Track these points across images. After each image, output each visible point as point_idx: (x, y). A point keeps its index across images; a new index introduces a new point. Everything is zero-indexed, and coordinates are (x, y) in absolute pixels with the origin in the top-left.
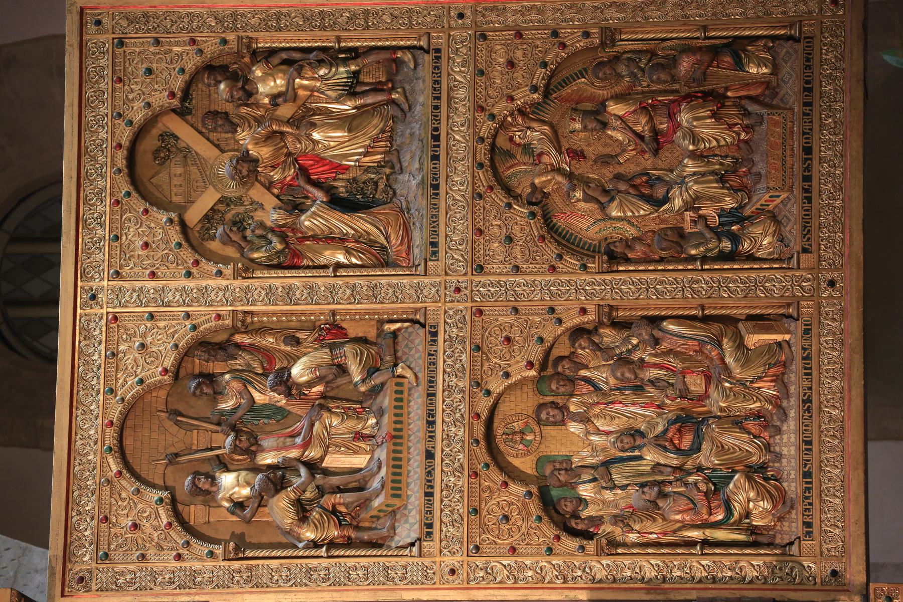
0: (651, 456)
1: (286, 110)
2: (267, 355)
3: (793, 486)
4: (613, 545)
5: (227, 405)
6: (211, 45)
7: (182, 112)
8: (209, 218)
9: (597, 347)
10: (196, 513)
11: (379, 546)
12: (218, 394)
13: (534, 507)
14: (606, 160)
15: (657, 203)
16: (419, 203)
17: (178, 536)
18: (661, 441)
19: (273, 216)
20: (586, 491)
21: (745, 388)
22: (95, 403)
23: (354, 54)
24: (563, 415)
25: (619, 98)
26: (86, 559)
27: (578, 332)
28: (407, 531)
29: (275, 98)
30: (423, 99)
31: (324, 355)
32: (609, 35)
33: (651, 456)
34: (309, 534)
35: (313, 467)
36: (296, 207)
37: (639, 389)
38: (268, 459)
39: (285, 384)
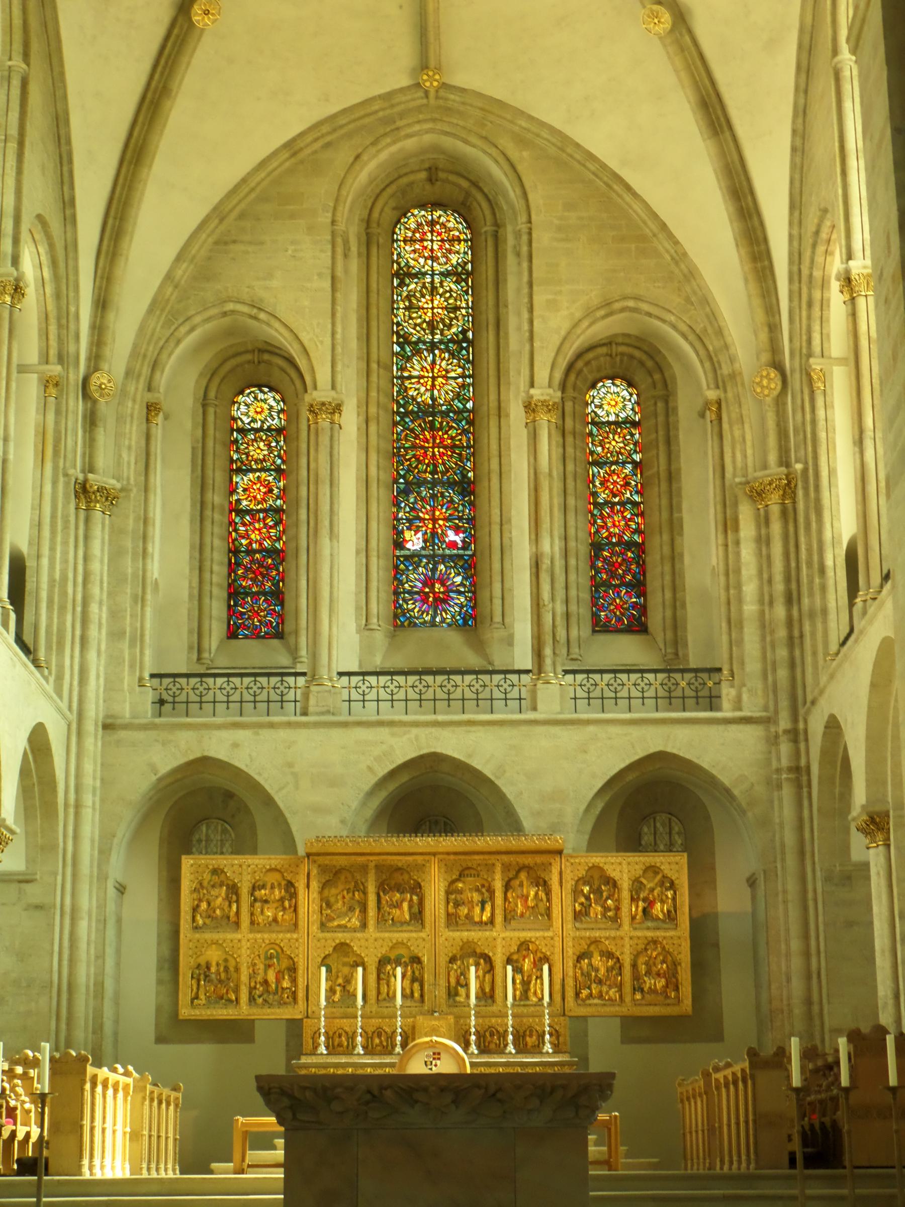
0: (593, 974)
1: (664, 898)
2: (613, 895)
3: (588, 1002)
4: (575, 966)
5: (603, 887)
6: (676, 882)
7: (663, 876)
8: (641, 883)
9: (615, 963)
10: (581, 882)
11: (575, 918)
12: (605, 885)
13: (583, 951)
14: (655, 964)
15: (645, 975)
16: (644, 926)
17: (576, 878)
18: (596, 976)
19: (641, 896)
20: (586, 961)
21: (607, 993)
22: (603, 860)
23: (676, 911)
24: (601, 956)
25: (667, 966)
26: (572, 861)
27: (618, 959)
28: (577, 925)
29: (667, 896)
30: (666, 926)
31: (612, 907)
32: (680, 964)
33: (593, 974)
34: (577, 905)
35: (590, 905)
36: (644, 900)
37: (607, 971)
38: (592, 896)
39: (607, 899)
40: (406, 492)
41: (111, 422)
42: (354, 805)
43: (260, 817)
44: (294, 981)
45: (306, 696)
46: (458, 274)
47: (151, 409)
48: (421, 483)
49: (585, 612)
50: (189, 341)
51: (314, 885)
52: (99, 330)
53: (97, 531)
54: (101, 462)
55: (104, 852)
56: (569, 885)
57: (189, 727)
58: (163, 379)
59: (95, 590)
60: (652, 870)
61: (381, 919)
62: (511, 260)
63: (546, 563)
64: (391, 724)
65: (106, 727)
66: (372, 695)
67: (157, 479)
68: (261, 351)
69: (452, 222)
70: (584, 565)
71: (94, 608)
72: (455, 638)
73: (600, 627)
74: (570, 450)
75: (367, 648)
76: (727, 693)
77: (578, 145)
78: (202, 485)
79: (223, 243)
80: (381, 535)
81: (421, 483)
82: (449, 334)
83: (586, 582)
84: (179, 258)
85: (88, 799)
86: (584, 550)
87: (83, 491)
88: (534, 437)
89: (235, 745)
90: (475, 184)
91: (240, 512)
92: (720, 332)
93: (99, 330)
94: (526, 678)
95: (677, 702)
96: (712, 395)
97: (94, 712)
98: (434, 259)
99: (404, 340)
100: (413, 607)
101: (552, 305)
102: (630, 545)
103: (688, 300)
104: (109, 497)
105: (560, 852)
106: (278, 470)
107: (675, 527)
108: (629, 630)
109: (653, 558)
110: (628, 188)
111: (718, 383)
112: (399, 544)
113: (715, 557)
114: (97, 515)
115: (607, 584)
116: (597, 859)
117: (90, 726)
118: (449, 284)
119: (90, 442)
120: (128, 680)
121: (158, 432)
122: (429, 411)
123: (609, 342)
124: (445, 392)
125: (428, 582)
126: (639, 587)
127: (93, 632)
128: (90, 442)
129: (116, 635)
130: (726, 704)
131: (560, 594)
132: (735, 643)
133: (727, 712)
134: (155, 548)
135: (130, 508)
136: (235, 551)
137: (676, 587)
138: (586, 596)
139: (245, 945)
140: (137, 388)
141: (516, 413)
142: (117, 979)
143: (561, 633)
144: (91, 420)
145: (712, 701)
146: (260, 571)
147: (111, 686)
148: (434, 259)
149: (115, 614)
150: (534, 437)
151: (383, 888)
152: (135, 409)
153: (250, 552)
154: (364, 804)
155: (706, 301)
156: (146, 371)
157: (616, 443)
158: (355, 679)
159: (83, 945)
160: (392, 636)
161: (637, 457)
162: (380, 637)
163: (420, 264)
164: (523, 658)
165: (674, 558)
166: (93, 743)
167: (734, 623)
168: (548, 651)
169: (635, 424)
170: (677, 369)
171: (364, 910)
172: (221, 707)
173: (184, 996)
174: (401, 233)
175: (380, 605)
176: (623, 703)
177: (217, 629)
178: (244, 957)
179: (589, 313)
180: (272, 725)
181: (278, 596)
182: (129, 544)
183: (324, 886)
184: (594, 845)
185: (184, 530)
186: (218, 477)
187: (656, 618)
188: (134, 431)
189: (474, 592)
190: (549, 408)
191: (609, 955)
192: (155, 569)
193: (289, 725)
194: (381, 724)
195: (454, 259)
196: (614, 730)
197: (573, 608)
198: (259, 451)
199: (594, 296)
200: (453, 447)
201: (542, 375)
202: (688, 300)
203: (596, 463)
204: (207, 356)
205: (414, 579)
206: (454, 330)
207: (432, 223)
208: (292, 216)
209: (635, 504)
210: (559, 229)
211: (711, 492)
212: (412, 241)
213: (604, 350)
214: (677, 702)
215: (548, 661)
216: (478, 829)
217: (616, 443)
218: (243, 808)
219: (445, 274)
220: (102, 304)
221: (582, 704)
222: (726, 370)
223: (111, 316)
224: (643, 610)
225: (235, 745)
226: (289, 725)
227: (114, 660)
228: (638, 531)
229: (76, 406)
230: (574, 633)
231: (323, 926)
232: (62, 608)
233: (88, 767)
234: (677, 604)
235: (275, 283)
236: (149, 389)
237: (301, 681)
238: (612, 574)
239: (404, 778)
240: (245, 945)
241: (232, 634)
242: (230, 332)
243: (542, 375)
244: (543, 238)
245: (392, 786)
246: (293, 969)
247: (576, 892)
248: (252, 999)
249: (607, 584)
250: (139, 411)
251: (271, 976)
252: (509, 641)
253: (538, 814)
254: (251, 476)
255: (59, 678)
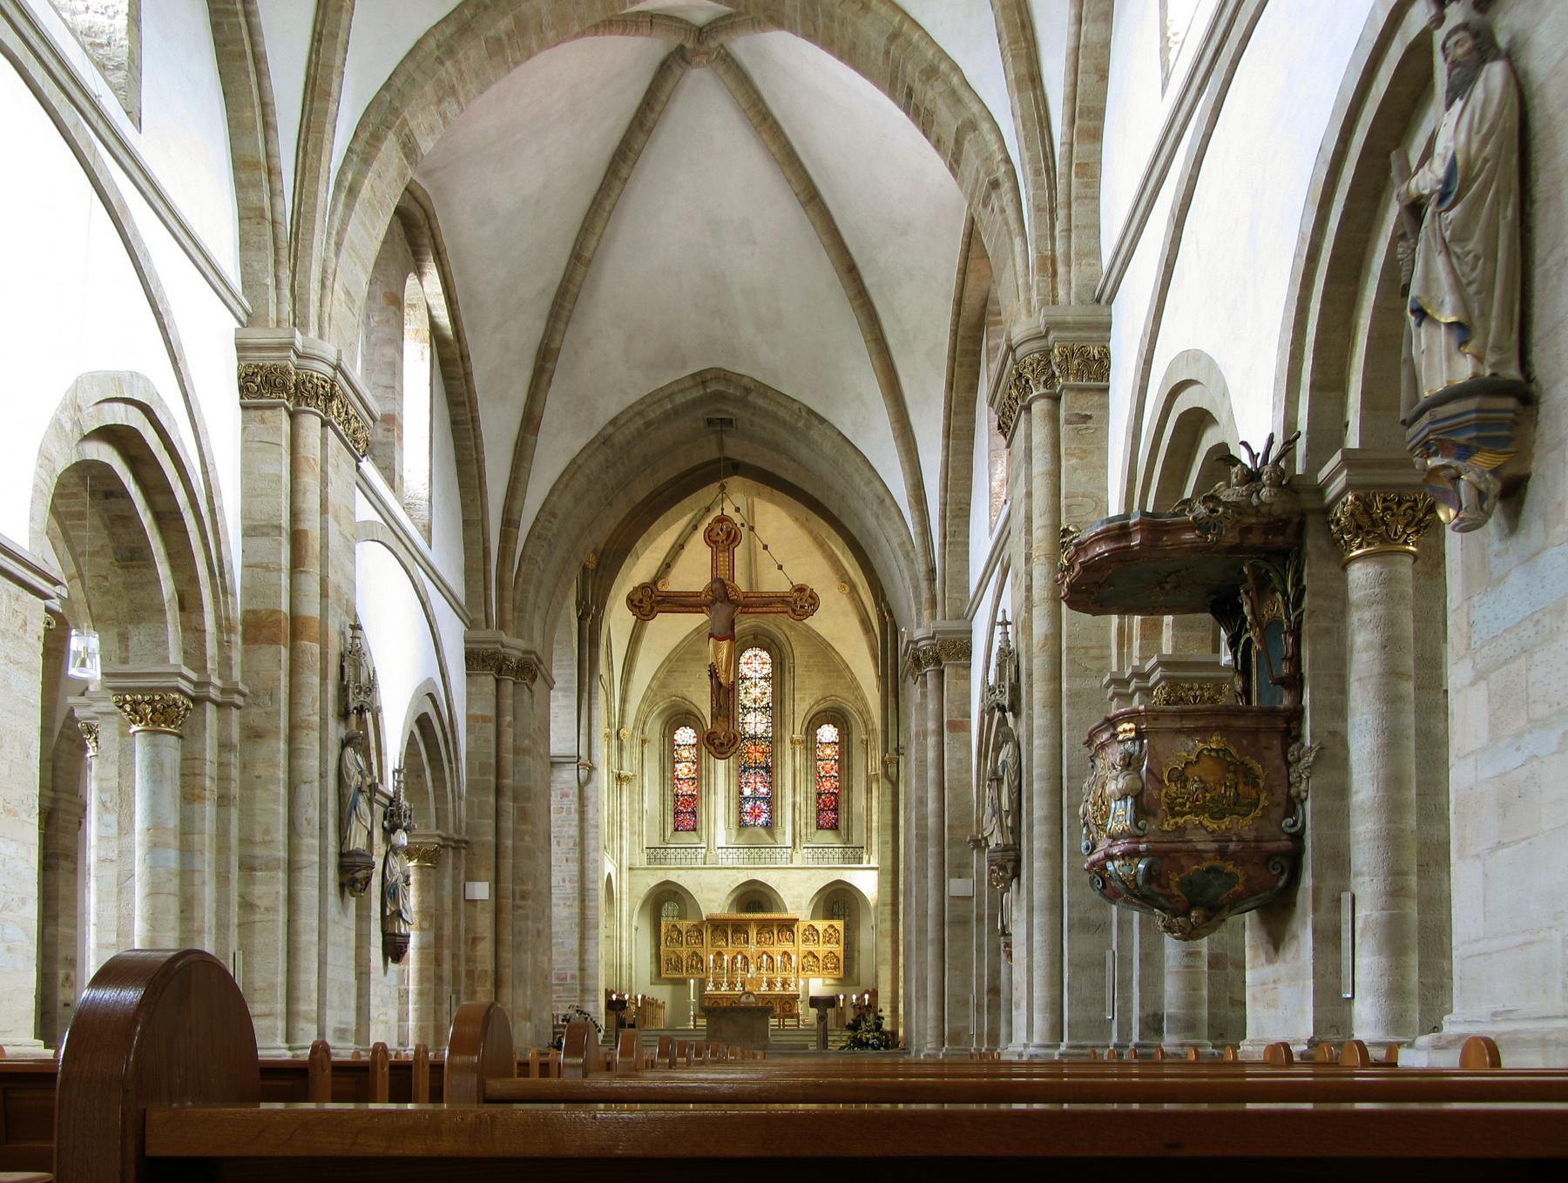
40: (744, 771)
41: (628, 748)
42: (724, 899)
43: (684, 896)
44: (702, 965)
45: (705, 857)
46: (765, 678)
47: (644, 742)
48: (750, 768)
49: (814, 822)
50: (656, 712)
51: (709, 931)
52: (623, 711)
53: (624, 793)
54: (625, 765)
55: (631, 916)
56: (801, 931)
57: (661, 869)
58: (647, 728)
59: (624, 817)
60: (831, 926)
61: (733, 942)
62: (787, 674)
63: (798, 805)
64: (738, 868)
65: (630, 869)
66: (731, 856)
67: (646, 770)
68: (686, 714)
69: (765, 655)
70: (814, 803)
71: (624, 824)
72: (762, 832)
73: (819, 827)
74: (809, 756)
75: (728, 835)
76: (865, 857)
77: (814, 631)
78: (663, 770)
79: (671, 671)
80: (734, 789)
81: (750, 768)
82: (763, 704)
83: (814, 809)
84: (653, 679)
85: (624, 897)
86: (814, 796)
87: (619, 778)
88: (794, 754)
89: (679, 876)
90: (773, 641)
91: (678, 779)
92: (868, 712)
93: (623, 711)
94: (789, 850)
95: (847, 860)
96: (864, 737)
97: (625, 864)
98: (756, 671)
99: (744, 707)
100: (747, 819)
101: (802, 699)
102: (833, 793)
103: (856, 698)
104: (628, 779)
105: (797, 920)
106: (693, 762)
107: (850, 788)
108: (831, 828)
109: (843, 799)
110: (834, 649)
111: (867, 732)
112: (741, 793)
113: (864, 802)
114: (624, 786)
115: (823, 810)
116: (812, 923)
117: (624, 869)
118: (762, 682)
119: (621, 757)
120: (637, 850)
121: (646, 750)
122: (754, 737)
123: (825, 711)
124: (760, 729)
125: (753, 808)
126: (835, 810)
127: (624, 833)
128: (621, 757)
129: (632, 833)
130: (865, 862)
131: (803, 815)
132: (869, 838)
133: (865, 865)
134: (646, 798)
135: (637, 783)
136: (677, 795)
137: (849, 812)
138: (814, 815)
139: (685, 953)
140: (638, 734)
141: (788, 741)
142: (636, 962)
143: (803, 832)
144: (621, 749)
145: (860, 860)
146: (686, 803)
147: (631, 854)
148: (756, 671)
149: (631, 825)
150: (794, 754)
151: (734, 932)
152: (637, 742)
153: (682, 796)
154: (728, 897)
155: (863, 698)
156: (641, 726)
157: (828, 751)
158: (724, 850)
159: (624, 950)
160: (739, 830)
161: (837, 757)
162: (734, 832)
163: (749, 674)
164: (789, 843)
165: (849, 801)
166: (625, 875)
167: (869, 830)
168: (798, 840)
169: (836, 743)
170: (853, 723)
171: (727, 940)
172: (673, 860)
173: (663, 970)
174: (742, 660)
175: (733, 819)
176: (826, 860)
177: (670, 828)
178: (684, 956)
179: (817, 702)
180: (692, 869)
181: (694, 813)
182: (636, 797)
183: (713, 931)
184: (813, 917)
185: (657, 788)
186: (668, 766)
187: (842, 824)
188: (637, 751)
189: (771, 813)
190: (800, 742)
191: (815, 957)
192: (646, 806)
193: (699, 868)
194: (734, 868)
195: (765, 672)
196: (821, 871)
197: (809, 821)
198: (685, 754)
199: (819, 695)
200: (763, 753)
201: (798, 729)
202: (856, 698)
203: (820, 760)
204: (664, 717)
205: (748, 807)
206: (764, 703)
207: (756, 656)
208: (698, 660)
209: (835, 777)
210: (806, 666)
211: (864, 775)
212: (747, 663)
213: (823, 714)
214: (847, 860)
215: (797, 844)
216: (771, 911)
217: (828, 751)
218: (682, 898)
219: (761, 678)
220: (624, 700)
221: (810, 860)
222: (870, 727)
223: (627, 705)
224: (837, 820)
225: (679, 876)
226: (699, 868)
227: (632, 843)
228: (836, 788)
229: (614, 742)
230: (809, 831)
231: (712, 946)
232: (613, 825)
233: (624, 885)
234: (849, 819)
235: (692, 689)
236: (643, 733)
237: (704, 850)
238: (825, 805)
239: (743, 889)
240: (685, 953)
241: (676, 830)
242: (673, 705)
243: (798, 729)
244: (799, 670)
245: (738, 892)
246: (702, 962)
247: (804, 934)
248: (687, 970)
249: (823, 810)
250: (639, 742)
251: (694, 963)
252: (784, 833)
253: (792, 903)
254: (683, 764)
255: (613, 851)
